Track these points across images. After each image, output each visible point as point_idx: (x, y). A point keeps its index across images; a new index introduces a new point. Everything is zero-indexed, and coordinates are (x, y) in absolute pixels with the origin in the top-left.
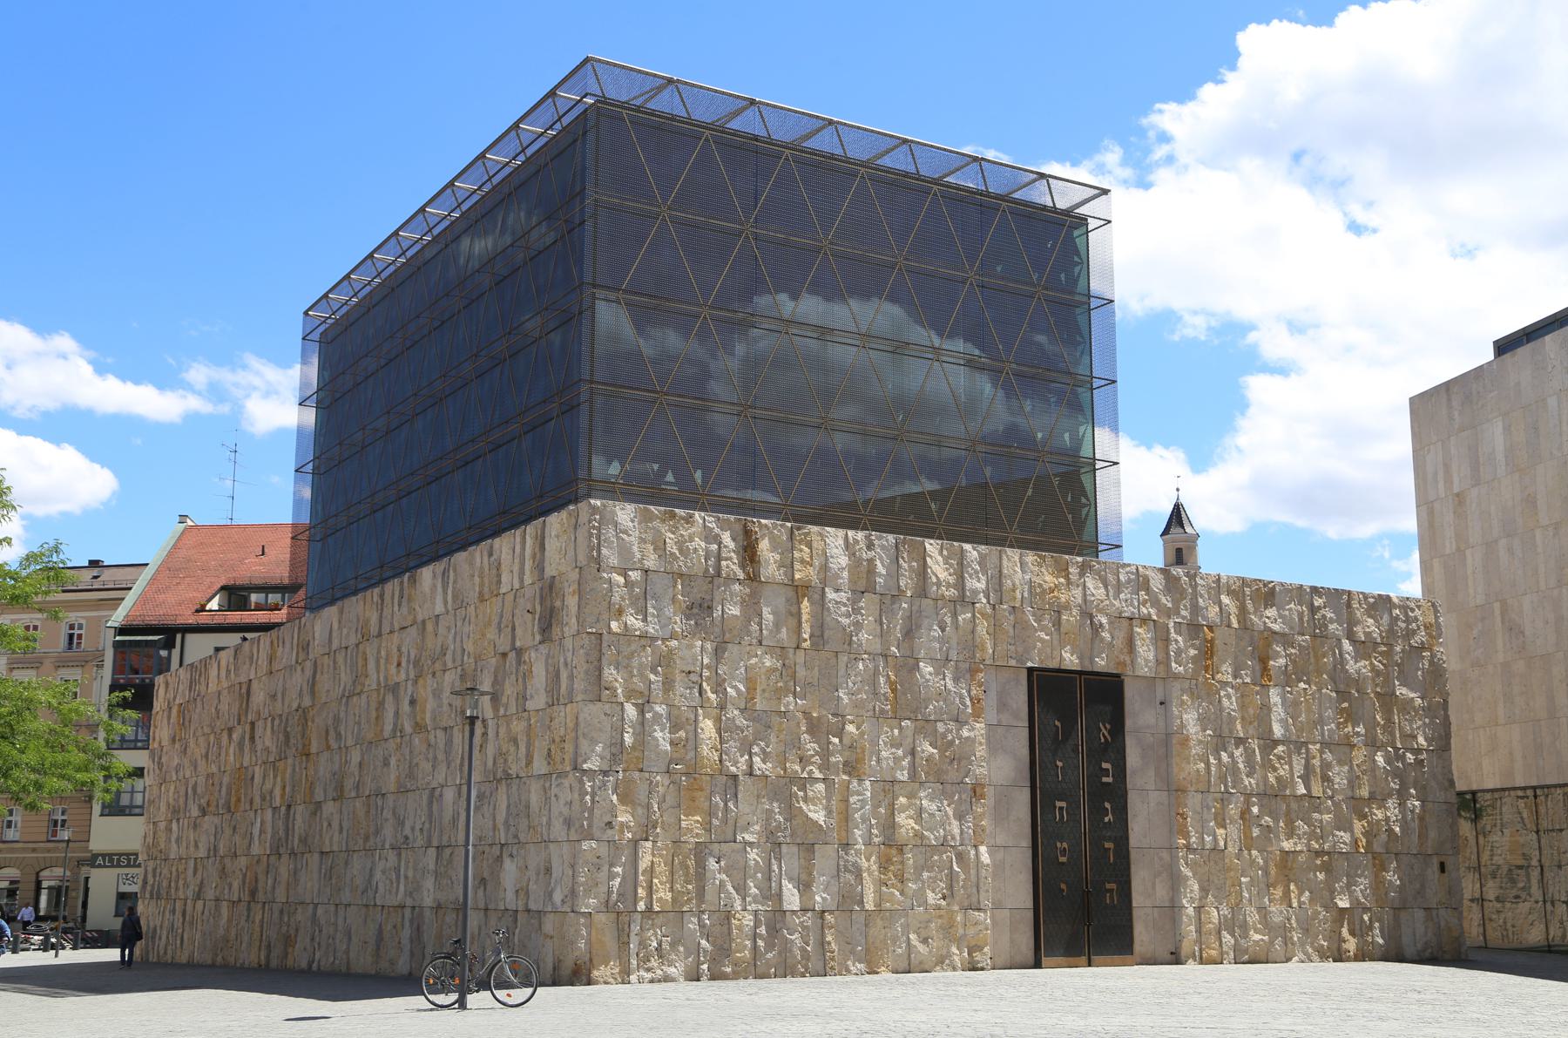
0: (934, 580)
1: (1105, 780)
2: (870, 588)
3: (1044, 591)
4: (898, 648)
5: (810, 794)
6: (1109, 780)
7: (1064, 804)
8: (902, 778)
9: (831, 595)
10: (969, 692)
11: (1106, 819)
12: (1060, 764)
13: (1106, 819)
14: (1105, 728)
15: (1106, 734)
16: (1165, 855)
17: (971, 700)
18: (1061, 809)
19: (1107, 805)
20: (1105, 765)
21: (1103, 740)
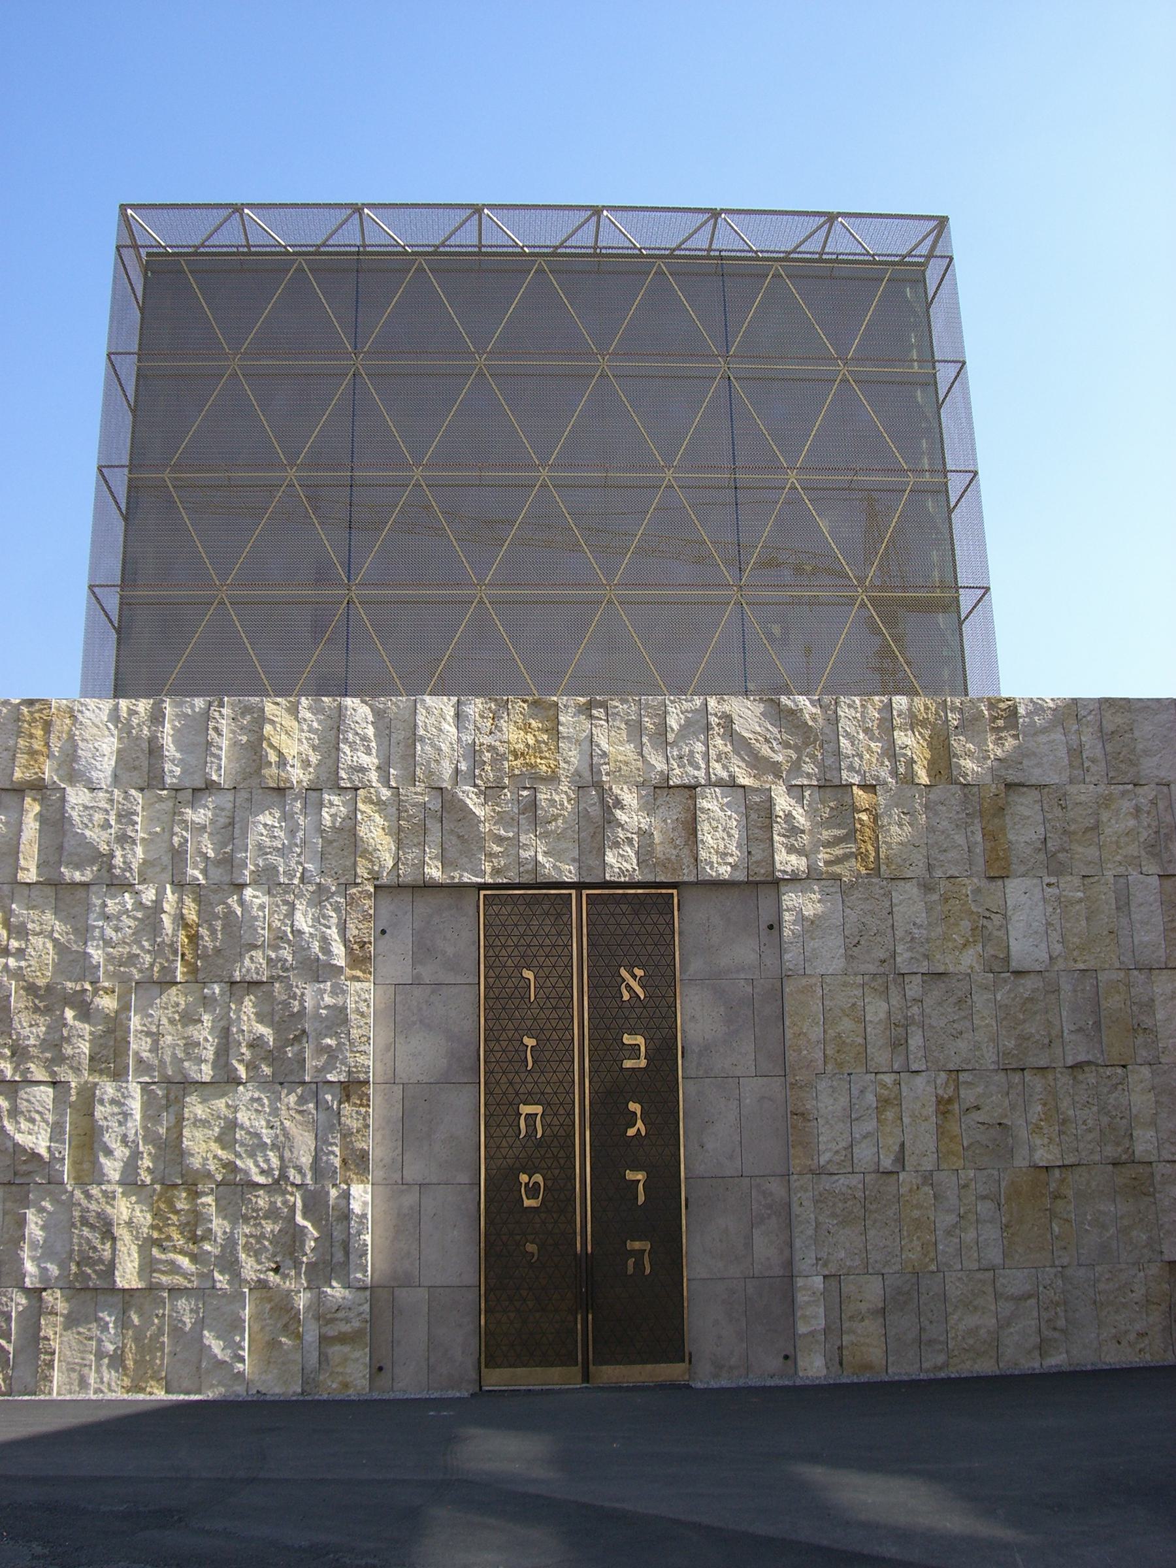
0: (273, 757)
1: (628, 1064)
2: (152, 780)
3: (498, 758)
4: (205, 872)
5: (23, 1105)
6: (643, 1063)
7: (538, 1109)
8: (197, 1077)
9: (77, 797)
10: (343, 929)
11: (631, 1132)
12: (530, 1042)
13: (631, 1132)
14: (634, 976)
15: (634, 984)
16: (776, 1187)
17: (345, 941)
18: (531, 1117)
19: (635, 1107)
20: (627, 1039)
21: (626, 996)
